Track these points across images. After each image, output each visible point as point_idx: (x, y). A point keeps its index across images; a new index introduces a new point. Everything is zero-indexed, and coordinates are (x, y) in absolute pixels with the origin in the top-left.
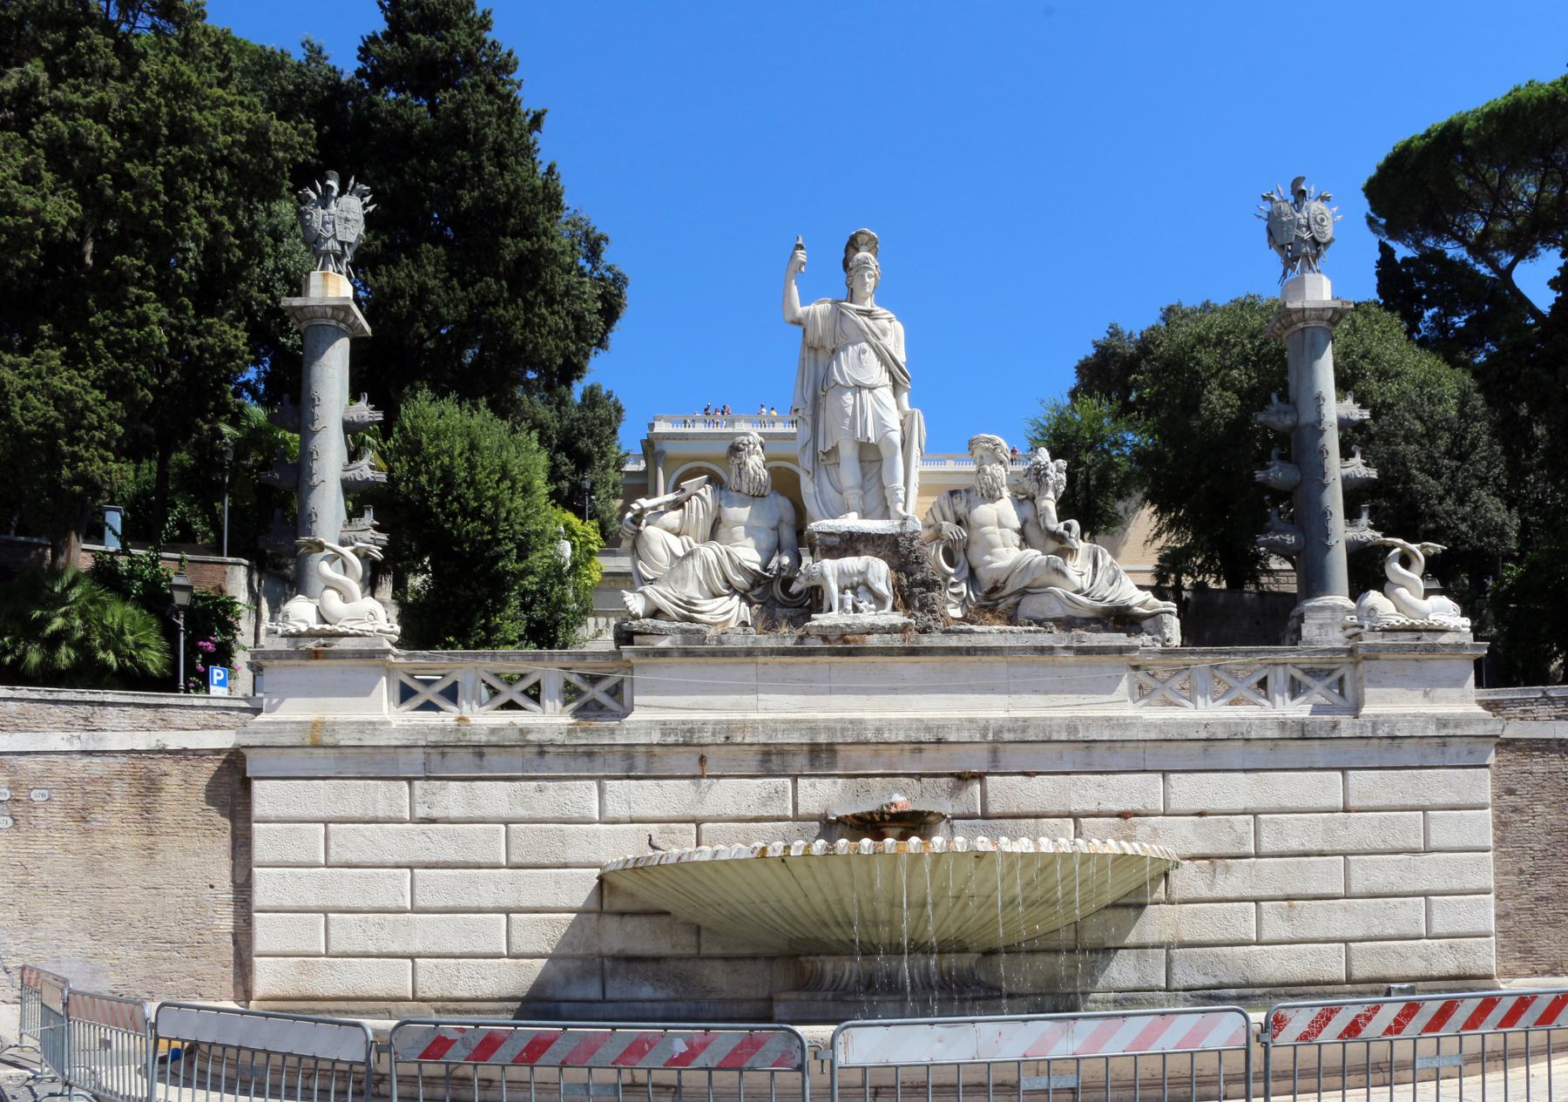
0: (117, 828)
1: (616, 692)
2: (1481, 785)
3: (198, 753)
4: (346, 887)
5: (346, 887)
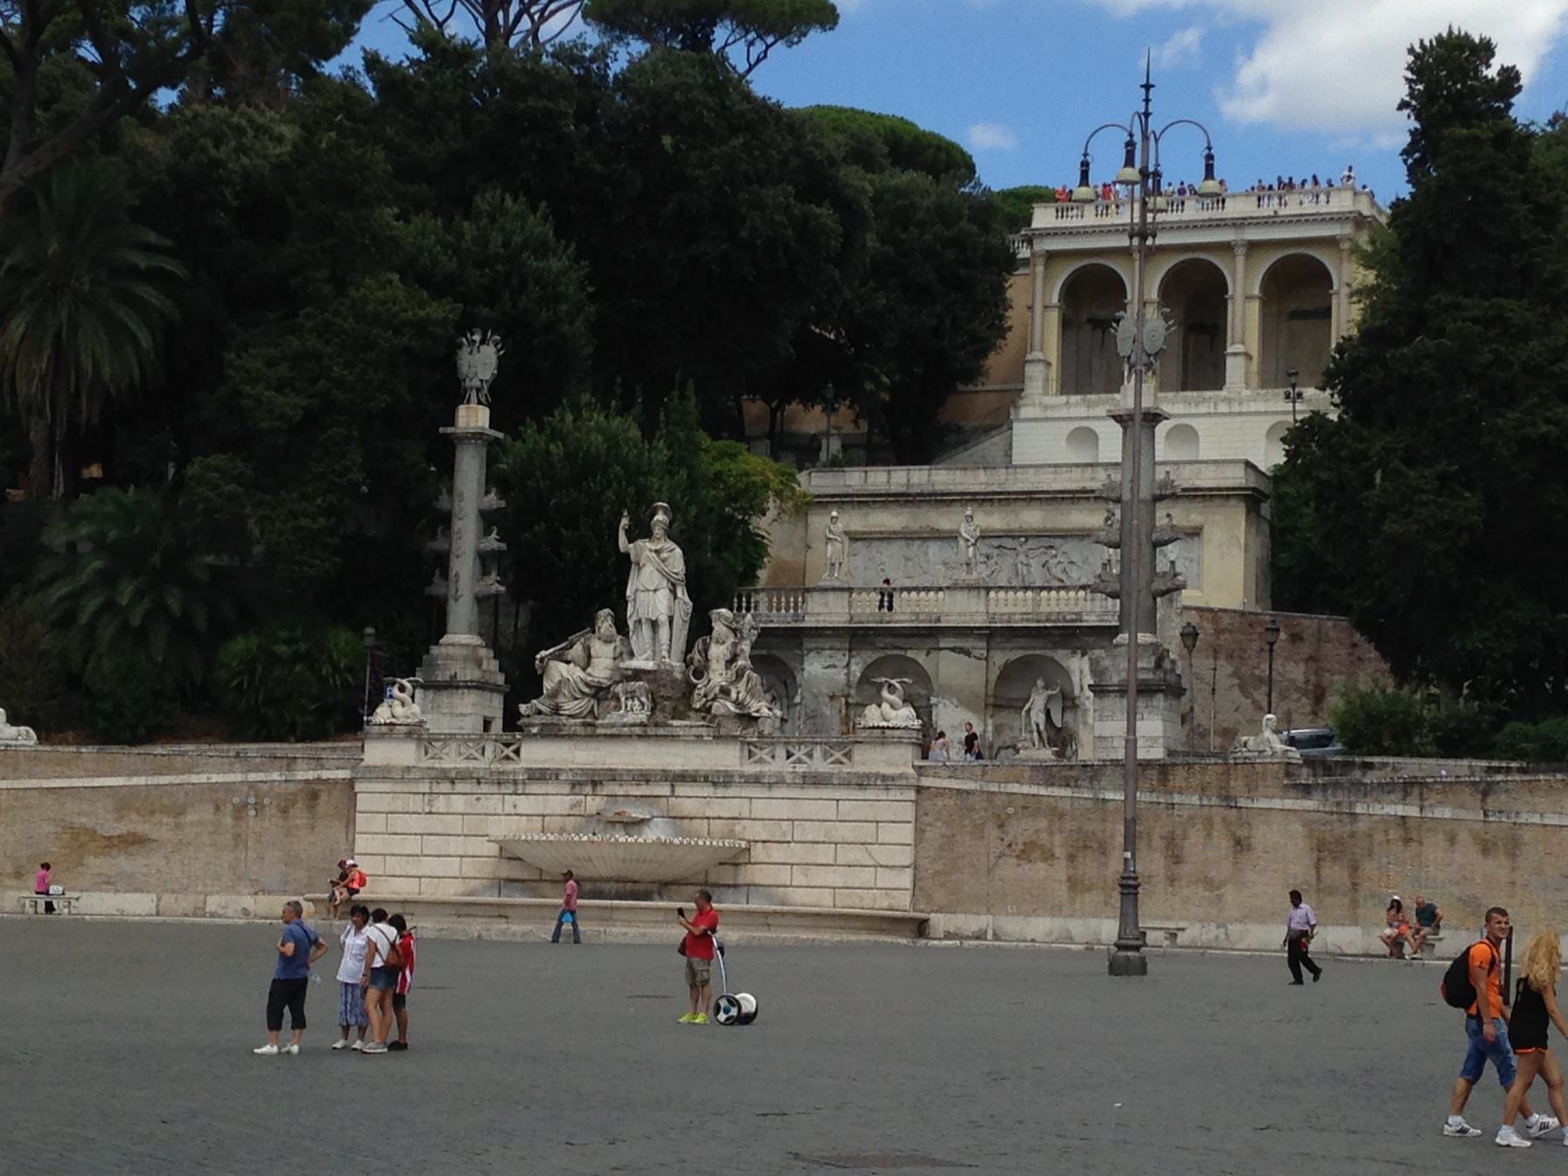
0: (299, 814)
1: (517, 752)
2: (908, 812)
3: (336, 782)
4: (396, 845)
5: (396, 845)
